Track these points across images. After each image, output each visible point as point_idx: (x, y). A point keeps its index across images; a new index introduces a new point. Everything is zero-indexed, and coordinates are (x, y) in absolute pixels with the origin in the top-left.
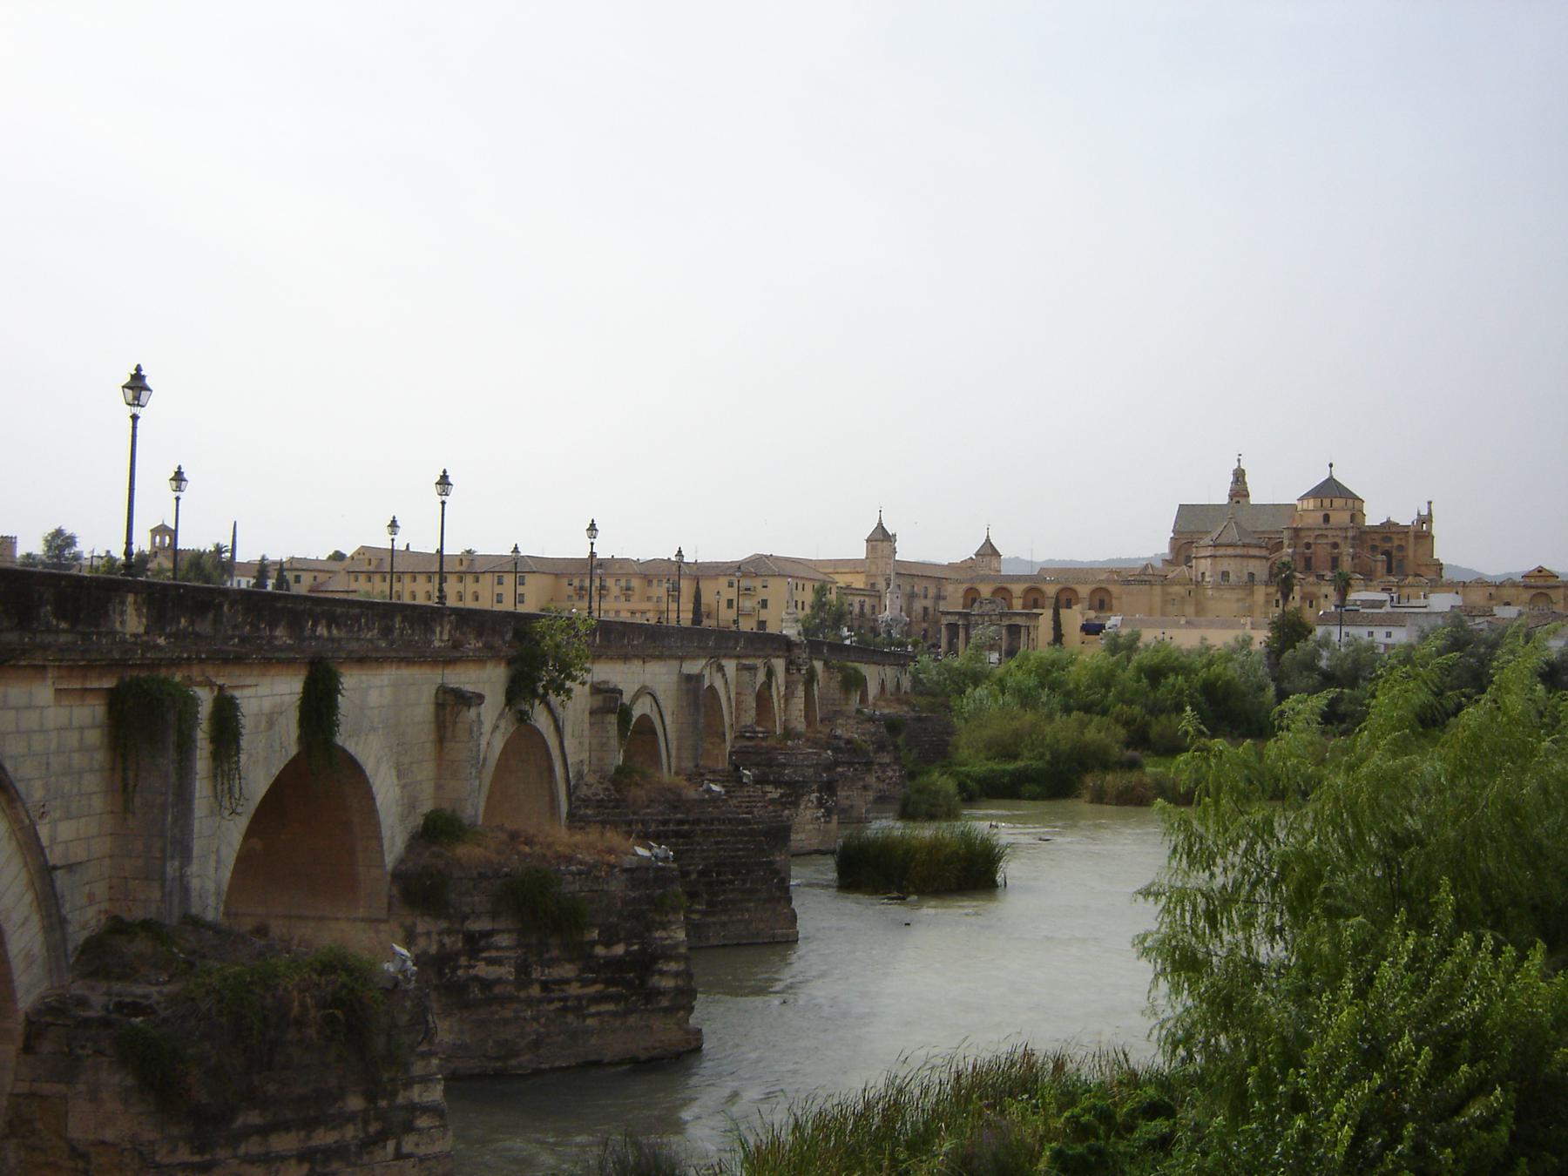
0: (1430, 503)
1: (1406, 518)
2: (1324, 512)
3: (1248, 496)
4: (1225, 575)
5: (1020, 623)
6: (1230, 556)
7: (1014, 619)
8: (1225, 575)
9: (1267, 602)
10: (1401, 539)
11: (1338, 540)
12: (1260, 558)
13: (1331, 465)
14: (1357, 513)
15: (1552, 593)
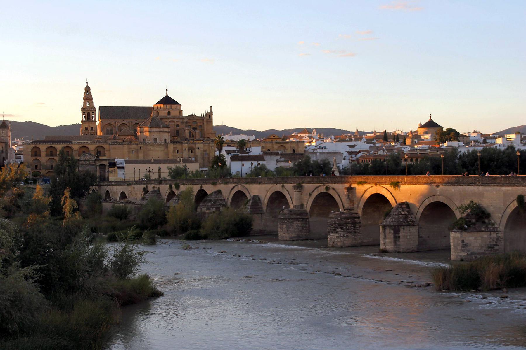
0: (211, 107)
1: (200, 112)
2: (166, 112)
3: (92, 99)
4: (155, 140)
5: (106, 164)
6: (157, 132)
7: (102, 162)
8: (155, 140)
9: (174, 151)
10: (200, 123)
11: (179, 123)
12: (168, 132)
13: (167, 90)
14: (181, 112)
15: (286, 145)
